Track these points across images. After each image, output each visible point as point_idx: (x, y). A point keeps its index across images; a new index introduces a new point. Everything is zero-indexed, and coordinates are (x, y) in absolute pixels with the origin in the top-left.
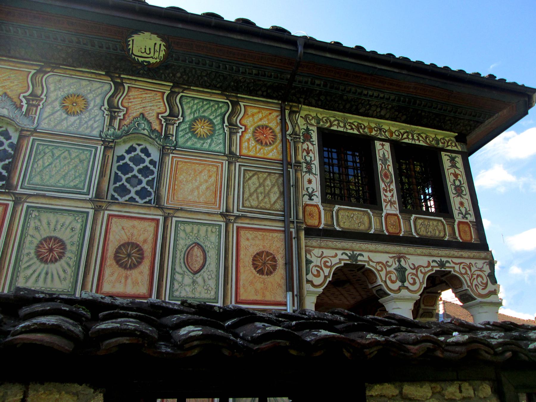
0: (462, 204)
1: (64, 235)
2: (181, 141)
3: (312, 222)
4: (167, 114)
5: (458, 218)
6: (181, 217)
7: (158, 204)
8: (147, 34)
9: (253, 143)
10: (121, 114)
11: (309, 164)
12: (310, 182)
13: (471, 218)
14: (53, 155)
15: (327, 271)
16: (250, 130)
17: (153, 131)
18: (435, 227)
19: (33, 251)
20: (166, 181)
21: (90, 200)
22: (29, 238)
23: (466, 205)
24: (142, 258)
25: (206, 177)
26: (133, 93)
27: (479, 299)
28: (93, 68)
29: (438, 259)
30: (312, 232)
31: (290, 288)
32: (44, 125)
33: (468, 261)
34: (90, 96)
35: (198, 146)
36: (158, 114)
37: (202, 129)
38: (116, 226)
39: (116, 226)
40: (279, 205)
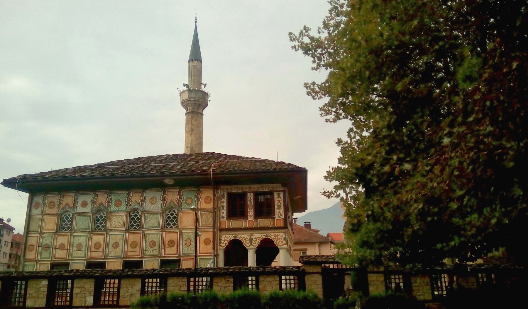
0: (279, 212)
1: (155, 240)
2: (183, 207)
3: (223, 226)
6: (184, 231)
7: (177, 227)
11: (223, 207)
12: (223, 213)
15: (226, 242)
20: (179, 220)
23: (281, 212)
26: (169, 193)
30: (221, 230)
31: (214, 248)
32: (147, 209)
33: (277, 234)
34: (157, 197)
37: (189, 201)
38: (168, 235)
39: (168, 235)
40: (212, 223)
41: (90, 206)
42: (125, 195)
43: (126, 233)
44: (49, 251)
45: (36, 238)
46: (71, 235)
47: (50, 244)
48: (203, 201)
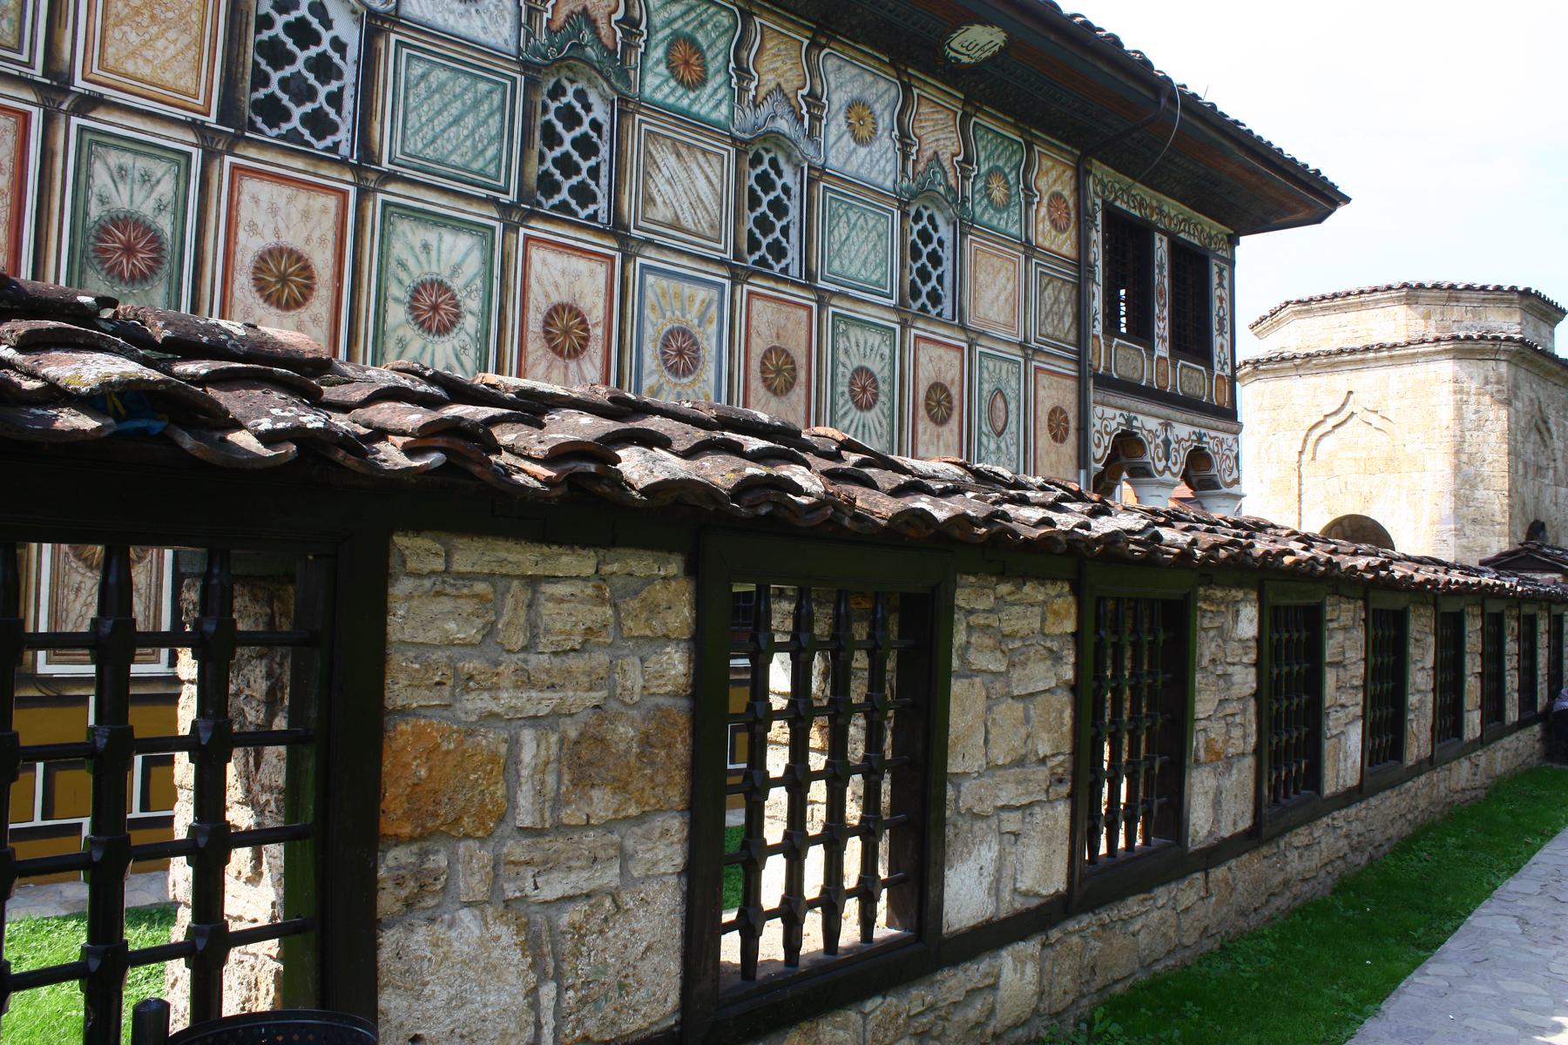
1: (875, 366)
2: (978, 210)
4: (960, 158)
5: (1217, 371)
8: (996, 29)
9: (1047, 223)
13: (1228, 371)
14: (848, 222)
16: (1045, 201)
17: (949, 188)
18: (1185, 377)
21: (894, 309)
22: (841, 369)
24: (951, 409)
25: (1004, 281)
27: (1225, 490)
28: (879, 50)
33: (1221, 435)
34: (878, 107)
35: (995, 222)
36: (953, 155)
40: (1072, 337)
42: (725, 20)
43: (738, 275)
46: (363, 194)
47: (165, 224)
48: (1043, 211)
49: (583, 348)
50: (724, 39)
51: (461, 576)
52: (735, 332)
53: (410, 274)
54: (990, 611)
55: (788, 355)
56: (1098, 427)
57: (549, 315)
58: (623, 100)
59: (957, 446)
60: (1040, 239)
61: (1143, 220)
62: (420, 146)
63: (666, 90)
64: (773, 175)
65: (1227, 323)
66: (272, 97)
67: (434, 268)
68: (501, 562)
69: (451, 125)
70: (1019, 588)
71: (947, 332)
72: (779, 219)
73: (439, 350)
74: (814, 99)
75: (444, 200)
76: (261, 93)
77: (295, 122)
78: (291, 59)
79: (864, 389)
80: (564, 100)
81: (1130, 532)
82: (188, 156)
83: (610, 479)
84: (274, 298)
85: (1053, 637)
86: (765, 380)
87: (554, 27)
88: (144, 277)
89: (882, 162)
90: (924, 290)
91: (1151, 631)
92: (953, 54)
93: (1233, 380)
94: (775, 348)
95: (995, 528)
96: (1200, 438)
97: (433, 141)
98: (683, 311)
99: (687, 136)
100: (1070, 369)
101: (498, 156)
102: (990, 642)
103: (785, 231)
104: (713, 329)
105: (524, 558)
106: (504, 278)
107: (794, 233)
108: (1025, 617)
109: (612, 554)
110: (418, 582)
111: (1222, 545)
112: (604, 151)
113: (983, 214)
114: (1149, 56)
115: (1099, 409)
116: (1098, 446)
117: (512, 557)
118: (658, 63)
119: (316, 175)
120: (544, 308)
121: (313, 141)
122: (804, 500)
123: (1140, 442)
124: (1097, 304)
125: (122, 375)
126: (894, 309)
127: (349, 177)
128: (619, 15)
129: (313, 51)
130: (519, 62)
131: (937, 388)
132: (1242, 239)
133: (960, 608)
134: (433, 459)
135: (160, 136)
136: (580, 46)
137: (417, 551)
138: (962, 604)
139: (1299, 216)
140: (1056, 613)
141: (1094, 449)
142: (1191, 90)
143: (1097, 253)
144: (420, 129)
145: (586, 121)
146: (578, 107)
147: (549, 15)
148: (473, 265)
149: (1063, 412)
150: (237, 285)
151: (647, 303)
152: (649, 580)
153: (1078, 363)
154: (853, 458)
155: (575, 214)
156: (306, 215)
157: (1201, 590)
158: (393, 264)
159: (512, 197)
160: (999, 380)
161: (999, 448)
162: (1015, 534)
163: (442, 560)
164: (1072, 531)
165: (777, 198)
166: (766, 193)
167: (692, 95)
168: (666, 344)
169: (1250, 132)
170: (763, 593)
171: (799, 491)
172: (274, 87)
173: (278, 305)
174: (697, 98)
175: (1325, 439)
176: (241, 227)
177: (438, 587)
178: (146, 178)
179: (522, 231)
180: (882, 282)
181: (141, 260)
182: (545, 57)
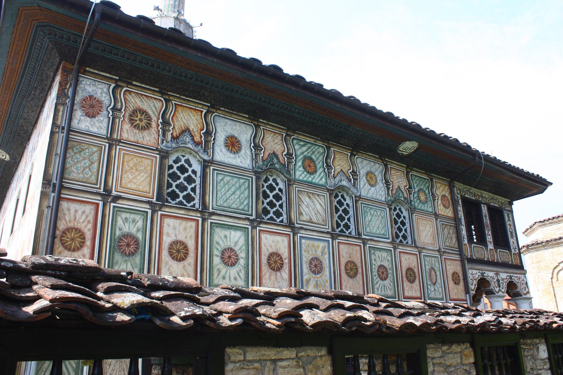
0: (513, 242)
1: (386, 264)
2: (416, 204)
4: (408, 187)
7: (414, 245)
9: (442, 206)
10: (391, 186)
13: (517, 251)
14: (371, 214)
16: (440, 198)
17: (405, 198)
18: (501, 255)
19: (376, 274)
21: (390, 243)
22: (374, 266)
24: (415, 277)
25: (429, 228)
27: (524, 296)
29: (509, 275)
32: (363, 194)
33: (519, 276)
34: (376, 173)
35: (423, 208)
36: (405, 186)
40: (456, 246)
41: (249, 152)
42: (321, 150)
43: (334, 237)
44: (138, 259)
45: (89, 209)
46: (204, 220)
47: (140, 236)
48: (440, 202)
49: (282, 267)
50: (322, 156)
51: (250, 361)
52: (335, 257)
53: (221, 246)
54: (441, 357)
55: (354, 263)
56: (471, 278)
57: (269, 257)
58: (289, 180)
59: (419, 290)
60: (440, 212)
61: (476, 200)
62: (222, 202)
63: (303, 176)
64: (343, 200)
65: (514, 233)
66: (173, 191)
67: (229, 244)
68: (263, 355)
69: (232, 195)
70: (450, 347)
71: (411, 249)
72: (346, 215)
73: (232, 272)
74: (354, 173)
75: (231, 220)
76: (170, 190)
77: (181, 198)
78: (179, 178)
79: (383, 273)
80: (269, 182)
81: (490, 321)
82: (147, 212)
83: (300, 323)
84: (175, 258)
85: (466, 365)
86: (347, 273)
87: (264, 159)
88: (133, 254)
89: (380, 192)
90: (401, 235)
91: (504, 358)
92: (400, 152)
93: (520, 254)
94: (349, 261)
95: (439, 326)
96: (511, 278)
97: (226, 201)
98: (315, 251)
99: (311, 190)
100: (457, 257)
101: (248, 204)
102: (442, 369)
103: (349, 219)
104: (327, 256)
105: (271, 353)
106: (253, 245)
107: (352, 220)
108: (454, 358)
109: (301, 349)
110: (235, 364)
111: (526, 323)
112: (284, 198)
113: (418, 206)
114: (469, 144)
115: (470, 271)
116: (472, 285)
117: (267, 353)
118: (300, 167)
119: (188, 215)
120: (267, 254)
121: (187, 204)
122: (368, 323)
123: (488, 282)
124: (464, 232)
125: (137, 301)
126: (390, 243)
127: (199, 215)
128: (286, 152)
129: (186, 175)
130: (253, 172)
131: (409, 270)
132: (514, 202)
133: (429, 357)
134: (239, 321)
135: (138, 207)
136: (273, 164)
137: (234, 353)
138: (430, 355)
139: (534, 192)
140: (466, 355)
141: (470, 286)
142: (486, 153)
143: (461, 214)
144: (222, 197)
145: (277, 189)
146: (274, 184)
147: (262, 155)
148: (242, 241)
149: (457, 273)
150: (163, 254)
151: (303, 249)
152: (315, 358)
153: (460, 255)
154: (384, 305)
155: (275, 221)
156: (185, 229)
157: (522, 341)
158: (215, 243)
159: (254, 217)
160: (432, 264)
161: (435, 289)
162: (446, 328)
163: (243, 356)
164: (468, 323)
165: (345, 208)
166: (341, 207)
167: (312, 176)
168: (311, 263)
169: (510, 165)
170: (356, 359)
171: (366, 320)
172: (174, 188)
173: (177, 260)
174: (314, 177)
175: (561, 272)
176: (164, 234)
177: (242, 366)
178: (134, 221)
179: (258, 228)
180: (385, 234)
181: (132, 249)
182: (262, 169)
